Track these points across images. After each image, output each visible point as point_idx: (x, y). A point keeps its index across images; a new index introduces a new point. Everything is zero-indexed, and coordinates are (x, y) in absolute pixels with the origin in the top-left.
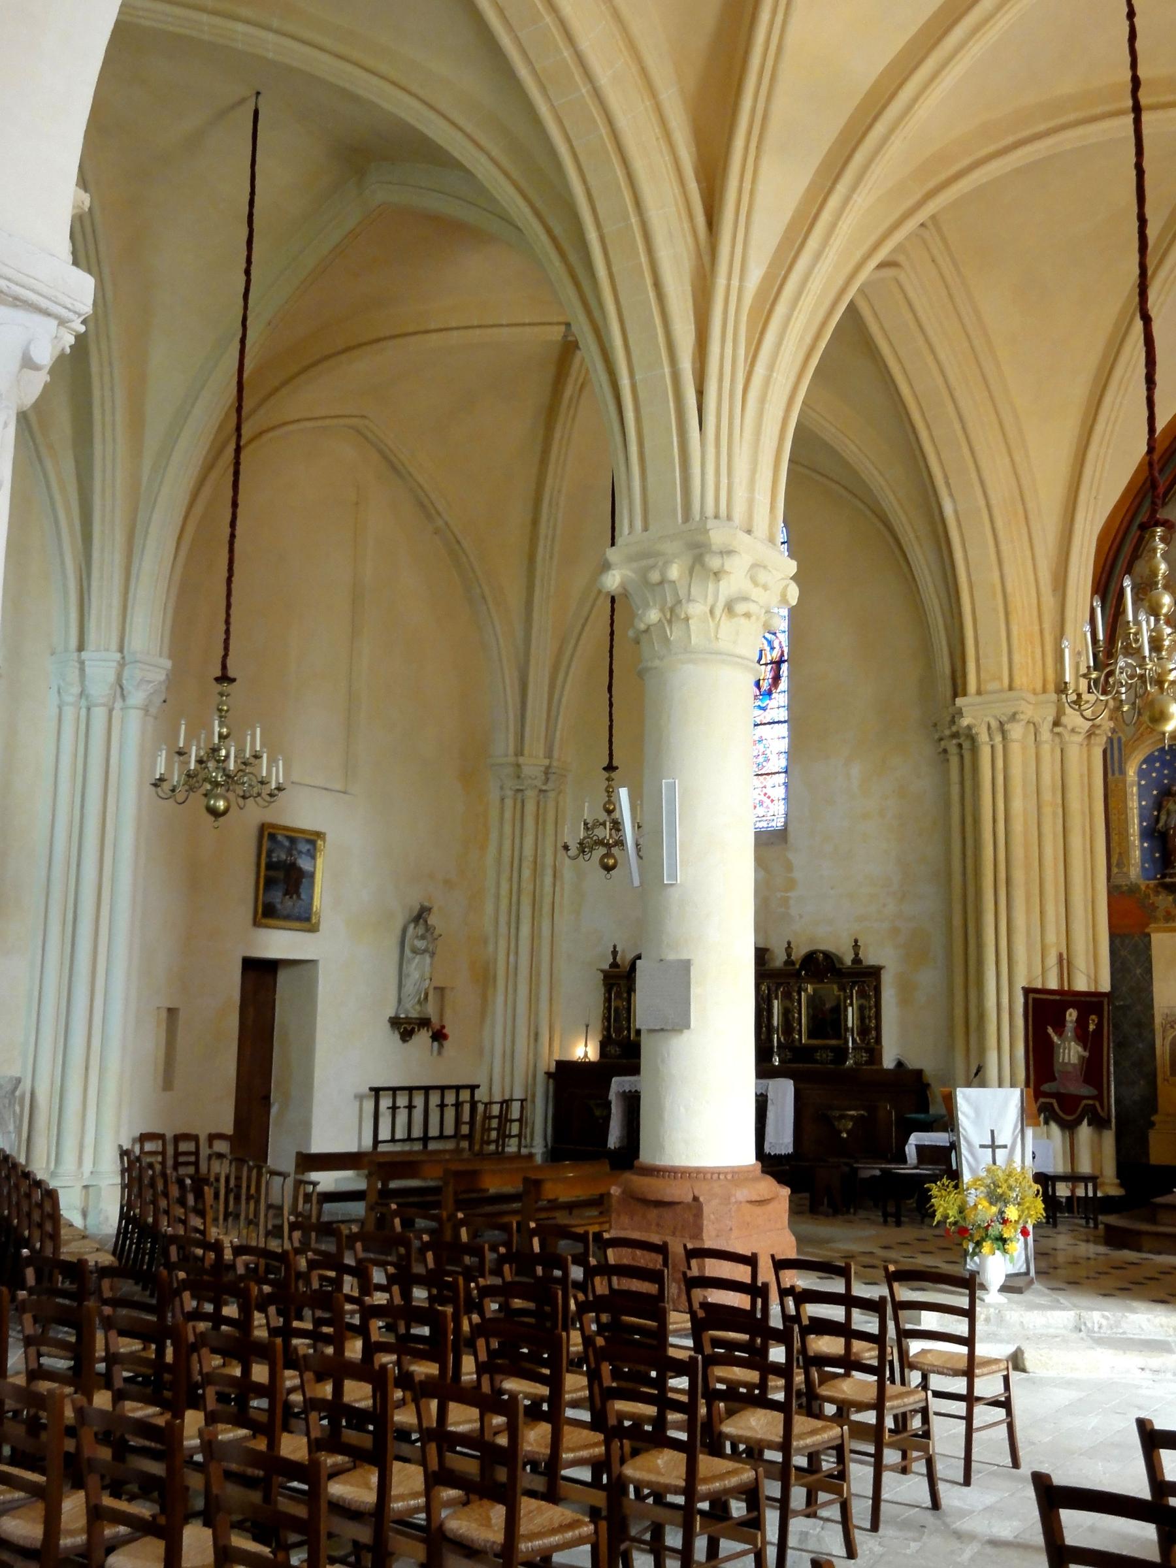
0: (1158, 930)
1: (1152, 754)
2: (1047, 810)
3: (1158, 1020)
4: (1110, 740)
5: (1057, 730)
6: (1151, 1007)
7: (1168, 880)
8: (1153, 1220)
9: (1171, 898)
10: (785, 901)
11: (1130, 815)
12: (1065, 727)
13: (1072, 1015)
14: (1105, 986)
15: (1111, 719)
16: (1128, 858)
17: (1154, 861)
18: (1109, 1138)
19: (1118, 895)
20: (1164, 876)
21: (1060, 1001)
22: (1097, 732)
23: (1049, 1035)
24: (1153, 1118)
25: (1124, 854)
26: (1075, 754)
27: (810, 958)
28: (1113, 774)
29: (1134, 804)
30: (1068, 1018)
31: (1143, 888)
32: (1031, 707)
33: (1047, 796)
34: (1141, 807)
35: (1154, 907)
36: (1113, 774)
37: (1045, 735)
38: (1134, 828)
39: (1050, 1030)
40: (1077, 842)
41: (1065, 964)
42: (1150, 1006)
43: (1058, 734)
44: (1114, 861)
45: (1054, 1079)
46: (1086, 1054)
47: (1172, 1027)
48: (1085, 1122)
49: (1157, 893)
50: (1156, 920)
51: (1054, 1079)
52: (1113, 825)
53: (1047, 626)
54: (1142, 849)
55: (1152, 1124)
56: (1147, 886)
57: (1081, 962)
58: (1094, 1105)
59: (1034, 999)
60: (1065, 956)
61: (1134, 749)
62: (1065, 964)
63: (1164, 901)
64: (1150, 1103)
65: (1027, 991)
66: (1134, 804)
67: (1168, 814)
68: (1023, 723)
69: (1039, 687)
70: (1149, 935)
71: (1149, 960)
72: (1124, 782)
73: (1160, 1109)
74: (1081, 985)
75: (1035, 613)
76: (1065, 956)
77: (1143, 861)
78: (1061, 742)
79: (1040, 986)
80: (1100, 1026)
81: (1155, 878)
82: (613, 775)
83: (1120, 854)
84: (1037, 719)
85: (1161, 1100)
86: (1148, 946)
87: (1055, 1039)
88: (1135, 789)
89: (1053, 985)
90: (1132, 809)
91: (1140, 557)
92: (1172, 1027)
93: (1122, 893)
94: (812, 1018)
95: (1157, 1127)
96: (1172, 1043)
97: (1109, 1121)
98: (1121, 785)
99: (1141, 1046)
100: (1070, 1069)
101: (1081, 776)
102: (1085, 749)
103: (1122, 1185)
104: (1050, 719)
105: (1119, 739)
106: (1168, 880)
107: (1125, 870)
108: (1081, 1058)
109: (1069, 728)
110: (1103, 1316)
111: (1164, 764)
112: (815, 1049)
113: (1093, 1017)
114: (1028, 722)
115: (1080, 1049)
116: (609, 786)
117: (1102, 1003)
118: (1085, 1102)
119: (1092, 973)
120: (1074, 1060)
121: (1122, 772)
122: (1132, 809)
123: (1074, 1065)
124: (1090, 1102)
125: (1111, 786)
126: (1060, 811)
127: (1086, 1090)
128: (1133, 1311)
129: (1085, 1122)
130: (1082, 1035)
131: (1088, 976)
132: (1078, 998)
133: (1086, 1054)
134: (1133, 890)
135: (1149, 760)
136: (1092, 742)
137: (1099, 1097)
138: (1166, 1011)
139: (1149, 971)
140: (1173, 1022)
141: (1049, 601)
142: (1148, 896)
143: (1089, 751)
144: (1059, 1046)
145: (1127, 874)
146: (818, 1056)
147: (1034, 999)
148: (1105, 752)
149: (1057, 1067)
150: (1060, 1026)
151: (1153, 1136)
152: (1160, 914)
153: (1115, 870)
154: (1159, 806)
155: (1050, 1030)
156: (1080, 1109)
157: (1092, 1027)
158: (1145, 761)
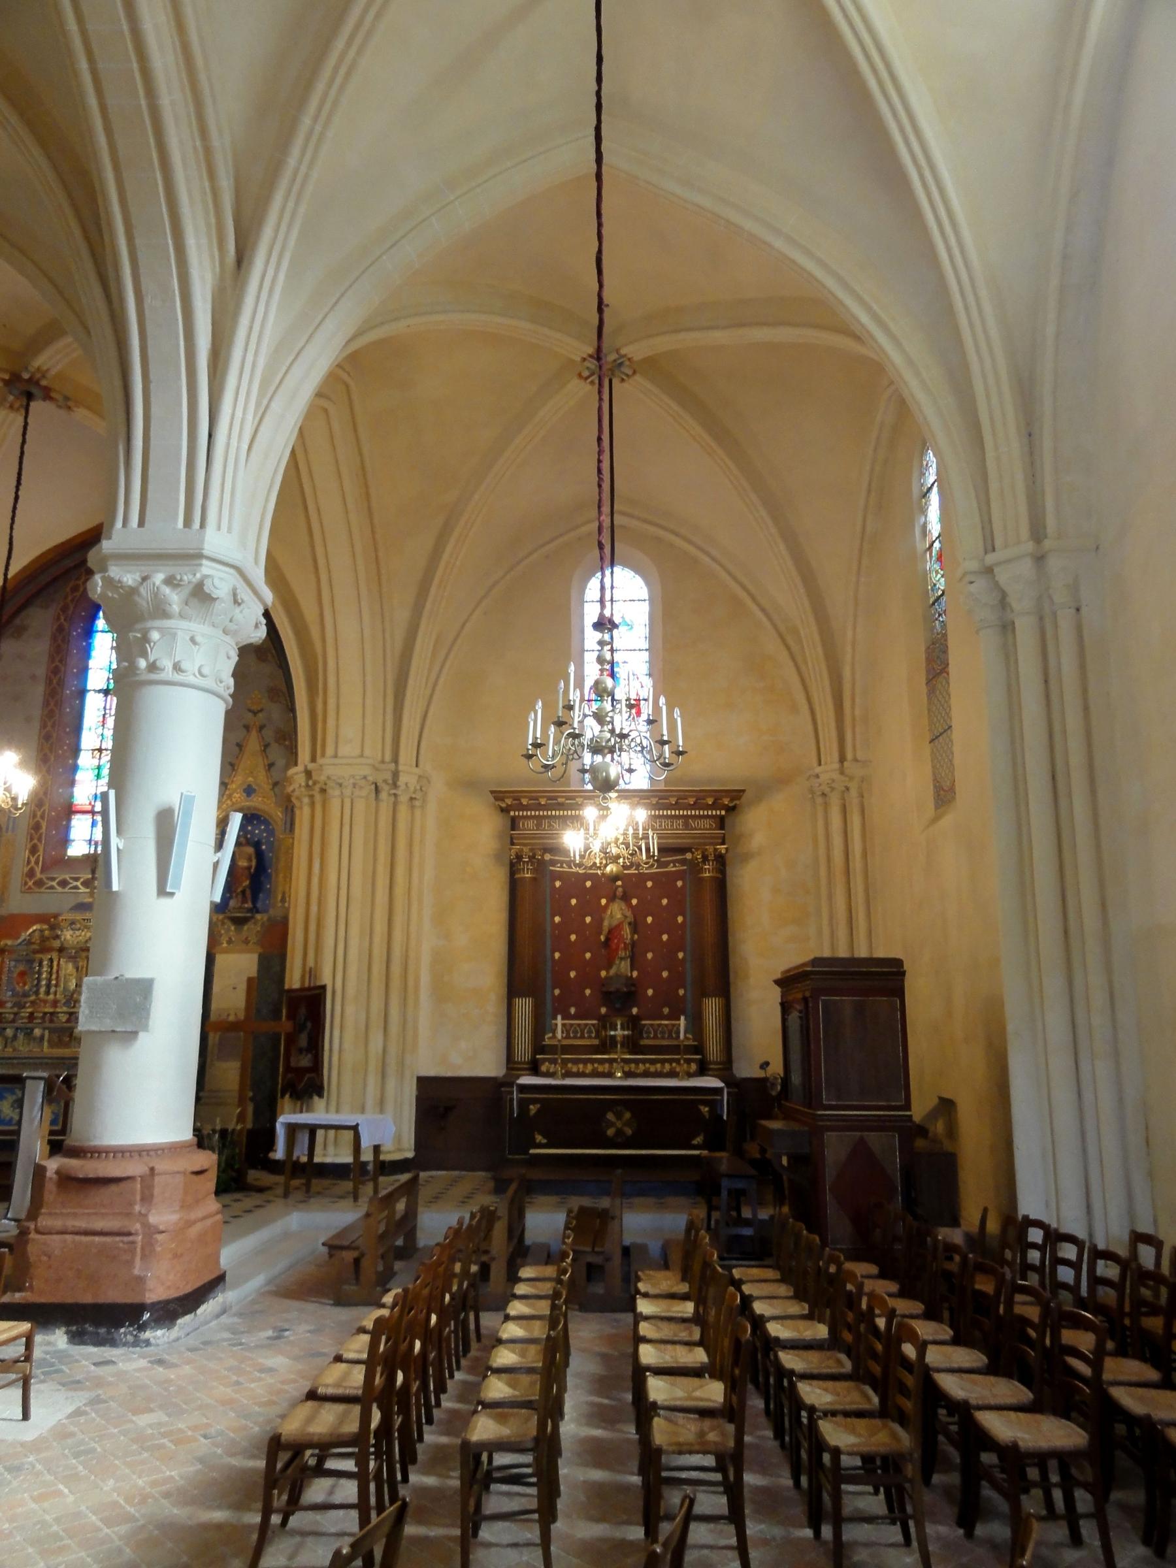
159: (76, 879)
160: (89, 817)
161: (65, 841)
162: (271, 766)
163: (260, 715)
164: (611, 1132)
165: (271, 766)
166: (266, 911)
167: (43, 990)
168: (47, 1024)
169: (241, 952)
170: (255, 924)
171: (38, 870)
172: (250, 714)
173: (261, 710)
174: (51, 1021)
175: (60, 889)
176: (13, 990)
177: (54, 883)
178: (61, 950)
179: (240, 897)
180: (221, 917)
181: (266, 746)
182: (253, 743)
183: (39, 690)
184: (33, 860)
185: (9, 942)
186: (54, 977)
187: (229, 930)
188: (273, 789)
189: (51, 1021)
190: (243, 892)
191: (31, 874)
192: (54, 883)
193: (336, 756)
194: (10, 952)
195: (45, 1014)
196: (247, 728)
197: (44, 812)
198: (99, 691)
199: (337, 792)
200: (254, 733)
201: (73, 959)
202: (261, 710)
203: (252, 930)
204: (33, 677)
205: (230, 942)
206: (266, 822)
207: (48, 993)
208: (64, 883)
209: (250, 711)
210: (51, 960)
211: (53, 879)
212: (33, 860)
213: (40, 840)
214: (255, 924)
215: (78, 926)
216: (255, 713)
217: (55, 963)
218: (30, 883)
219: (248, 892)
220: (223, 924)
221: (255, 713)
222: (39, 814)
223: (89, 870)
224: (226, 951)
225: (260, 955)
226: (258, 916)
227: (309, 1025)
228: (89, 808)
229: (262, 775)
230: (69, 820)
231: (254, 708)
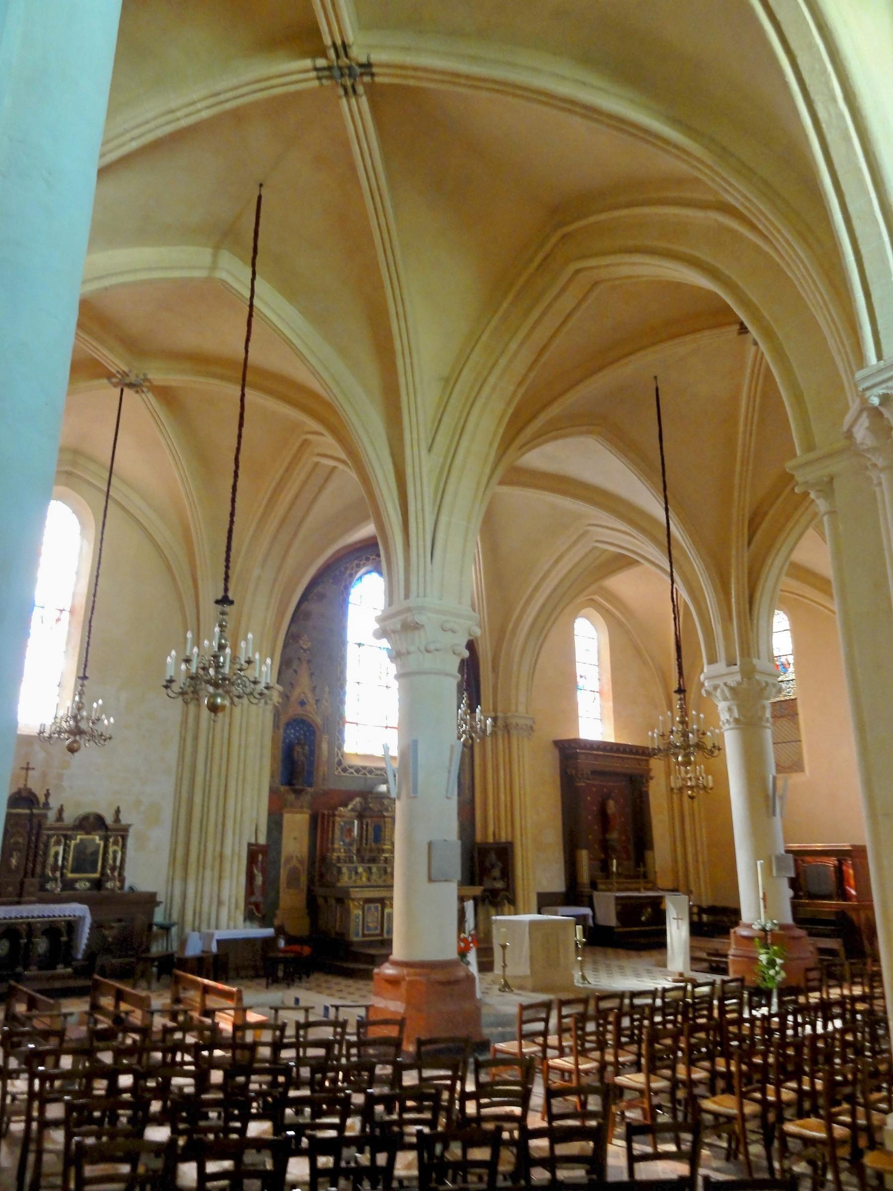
3: (283, 859)
10: (60, 777)
13: (260, 857)
19: (273, 791)
27: (85, 818)
42: (279, 853)
63: (291, 797)
65: (250, 845)
82: (86, 682)
94: (75, 859)
112: (76, 881)
116: (82, 690)
139: (281, 833)
140: (289, 859)
146: (77, 886)
164: (643, 918)
185: (342, 809)
227: (500, 865)
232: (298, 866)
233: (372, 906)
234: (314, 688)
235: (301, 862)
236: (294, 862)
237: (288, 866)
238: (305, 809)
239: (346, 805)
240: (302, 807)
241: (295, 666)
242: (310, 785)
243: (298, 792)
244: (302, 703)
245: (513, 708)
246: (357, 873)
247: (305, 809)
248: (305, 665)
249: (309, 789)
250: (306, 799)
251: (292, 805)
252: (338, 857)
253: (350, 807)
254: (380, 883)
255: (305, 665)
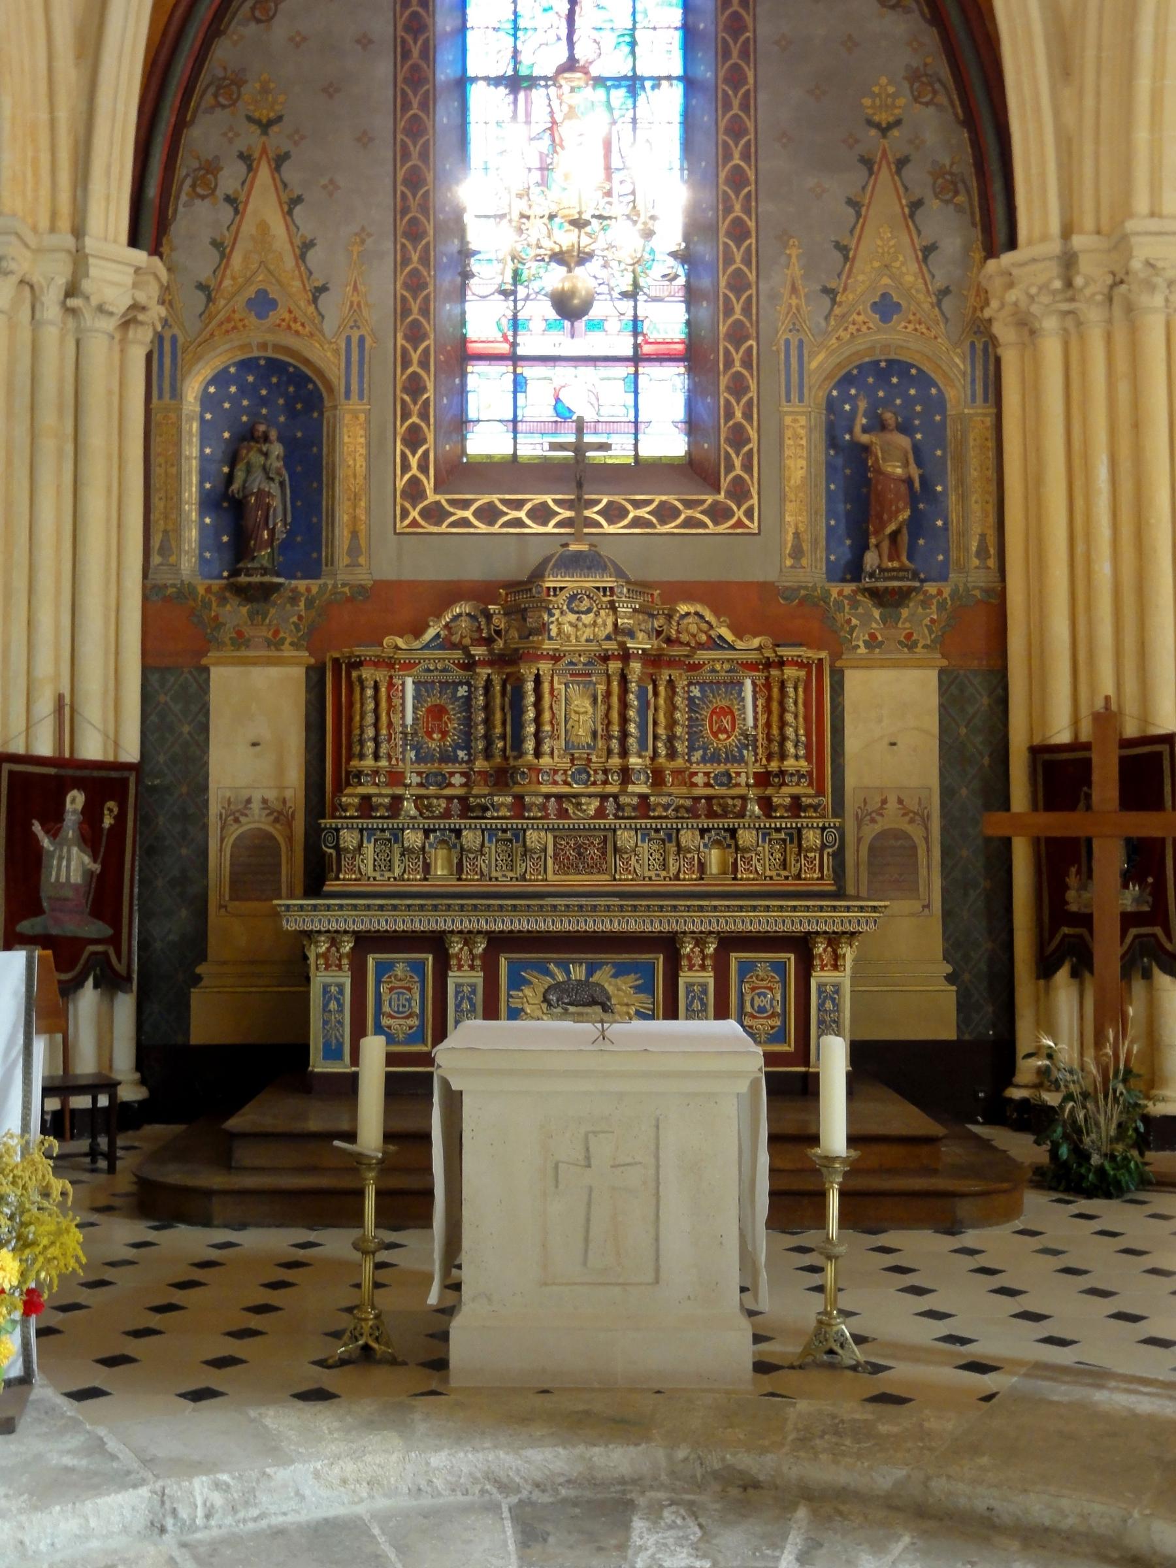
0: (219, 663)
1: (225, 370)
2: (48, 445)
3: (214, 809)
4: (159, 338)
5: (72, 302)
6: (205, 788)
7: (243, 579)
8: (225, 1162)
9: (244, 610)
11: (185, 468)
12: (87, 298)
13: (75, 801)
14: (131, 752)
15: (162, 302)
16: (179, 538)
17: (220, 547)
18: (125, 1006)
20: (235, 573)
21: (56, 777)
22: (141, 317)
23: (34, 837)
24: (199, 970)
25: (173, 533)
26: (99, 351)
28: (160, 397)
29: (192, 450)
30: (68, 806)
31: (201, 591)
32: (28, 254)
33: (48, 418)
34: (203, 457)
35: (218, 624)
36: (160, 397)
37: (51, 310)
38: (191, 492)
39: (37, 827)
40: (96, 505)
41: (66, 712)
42: (202, 788)
43: (73, 312)
44: (156, 542)
45: (38, 911)
46: (97, 867)
47: (237, 820)
48: (90, 982)
49: (223, 601)
50: (220, 645)
51: (38, 911)
52: (156, 482)
53: (63, 115)
54: (202, 527)
55: (197, 979)
56: (208, 590)
57: (93, 711)
58: (106, 954)
59: (11, 773)
60: (67, 700)
61: (198, 358)
62: (66, 712)
63: (235, 613)
64: (195, 946)
66: (192, 450)
67: (248, 472)
68: (13, 279)
69: (44, 223)
70: (206, 670)
71: (205, 710)
72: (179, 410)
73: (209, 958)
74: (92, 749)
75: (42, 87)
76: (67, 700)
77: (202, 548)
78: (78, 329)
79: (21, 750)
80: (121, 819)
81: (221, 577)
83: (165, 532)
84: (36, 278)
85: (212, 940)
86: (204, 688)
87: (46, 843)
88: (195, 426)
89: (44, 748)
90: (189, 458)
91: (224, 32)
92: (237, 820)
93: (167, 599)
95: (202, 984)
96: (234, 846)
97: (129, 979)
98: (173, 415)
99: (184, 851)
100: (70, 894)
101: (110, 393)
102: (117, 348)
103: (143, 1082)
104: (61, 281)
105: (174, 339)
106: (243, 579)
107: (172, 559)
108: (88, 874)
109: (94, 301)
110: (217, 1485)
111: (243, 390)
113: (111, 804)
114: (22, 282)
115: (87, 859)
117: (124, 782)
118: (92, 948)
119: (110, 731)
120: (76, 878)
121: (176, 394)
122: (189, 458)
123: (76, 887)
124: (100, 948)
125: (157, 417)
126: (69, 448)
127: (97, 929)
128: (274, 1451)
129: (90, 982)
130: (91, 836)
131: (106, 736)
132: (86, 773)
133: (97, 867)
134: (185, 593)
135: (220, 379)
136: (131, 334)
137: (115, 940)
138: (228, 794)
139: (205, 728)
140: (236, 812)
141: (68, 72)
142: (207, 605)
143: (122, 351)
144: (51, 855)
145: (176, 568)
147: (11, 773)
148: (149, 357)
149: (46, 892)
150: (54, 818)
151: (197, 997)
152: (226, 634)
153: (156, 559)
154: (233, 460)
155: (37, 827)
156: (82, 961)
157: (108, 822)
158: (213, 381)
159: (518, 505)
160: (506, 368)
161: (461, 424)
162: (928, 251)
163: (895, 133)
165: (928, 251)
166: (945, 579)
167: (530, 745)
168: (554, 821)
169: (897, 665)
170: (925, 604)
171: (429, 485)
172: (873, 132)
173: (898, 123)
174: (563, 814)
175: (483, 528)
176: (417, 748)
177: (468, 514)
178: (556, 658)
179: (886, 545)
180: (849, 588)
181: (916, 205)
182: (885, 200)
183: (383, 69)
184: (414, 462)
185: (400, 642)
186: (547, 716)
187: (867, 619)
188: (939, 304)
189: (563, 814)
190: (894, 536)
191: (414, 491)
192: (468, 514)
193: (1152, 214)
194: (408, 666)
195: (547, 796)
196: (868, 163)
197: (426, 351)
198: (497, 81)
199: (1158, 300)
200: (885, 175)
201: (580, 676)
202: (898, 123)
203: (919, 618)
204: (365, 41)
205: (872, 642)
206: (924, 380)
207: (538, 754)
208: (489, 514)
209: (870, 123)
210: (538, 680)
211: (465, 504)
212: (414, 462)
213: (424, 416)
214: (925, 604)
215: (586, 603)
216: (884, 130)
217: (546, 687)
218: (414, 514)
219: (904, 538)
220: (855, 604)
221: (884, 130)
222: (415, 357)
223: (574, 484)
224: (866, 665)
225: (942, 672)
226: (931, 588)
228: (504, 348)
229: (909, 271)
230: (463, 375)
231: (883, 118)
232: (276, 831)
233: (401, 963)
234: (308, 245)
235: (280, 816)
236: (256, 820)
237: (234, 832)
238: (288, 652)
239: (418, 633)
240: (275, 643)
241: (228, 181)
242: (313, 571)
243: (258, 596)
244: (263, 304)
245: (1142, 204)
246: (526, 851)
247: (288, 652)
248: (264, 173)
249: (301, 584)
250: (286, 615)
251: (240, 640)
252: (366, 798)
253: (430, 633)
254: (505, 880)
255: (264, 173)
